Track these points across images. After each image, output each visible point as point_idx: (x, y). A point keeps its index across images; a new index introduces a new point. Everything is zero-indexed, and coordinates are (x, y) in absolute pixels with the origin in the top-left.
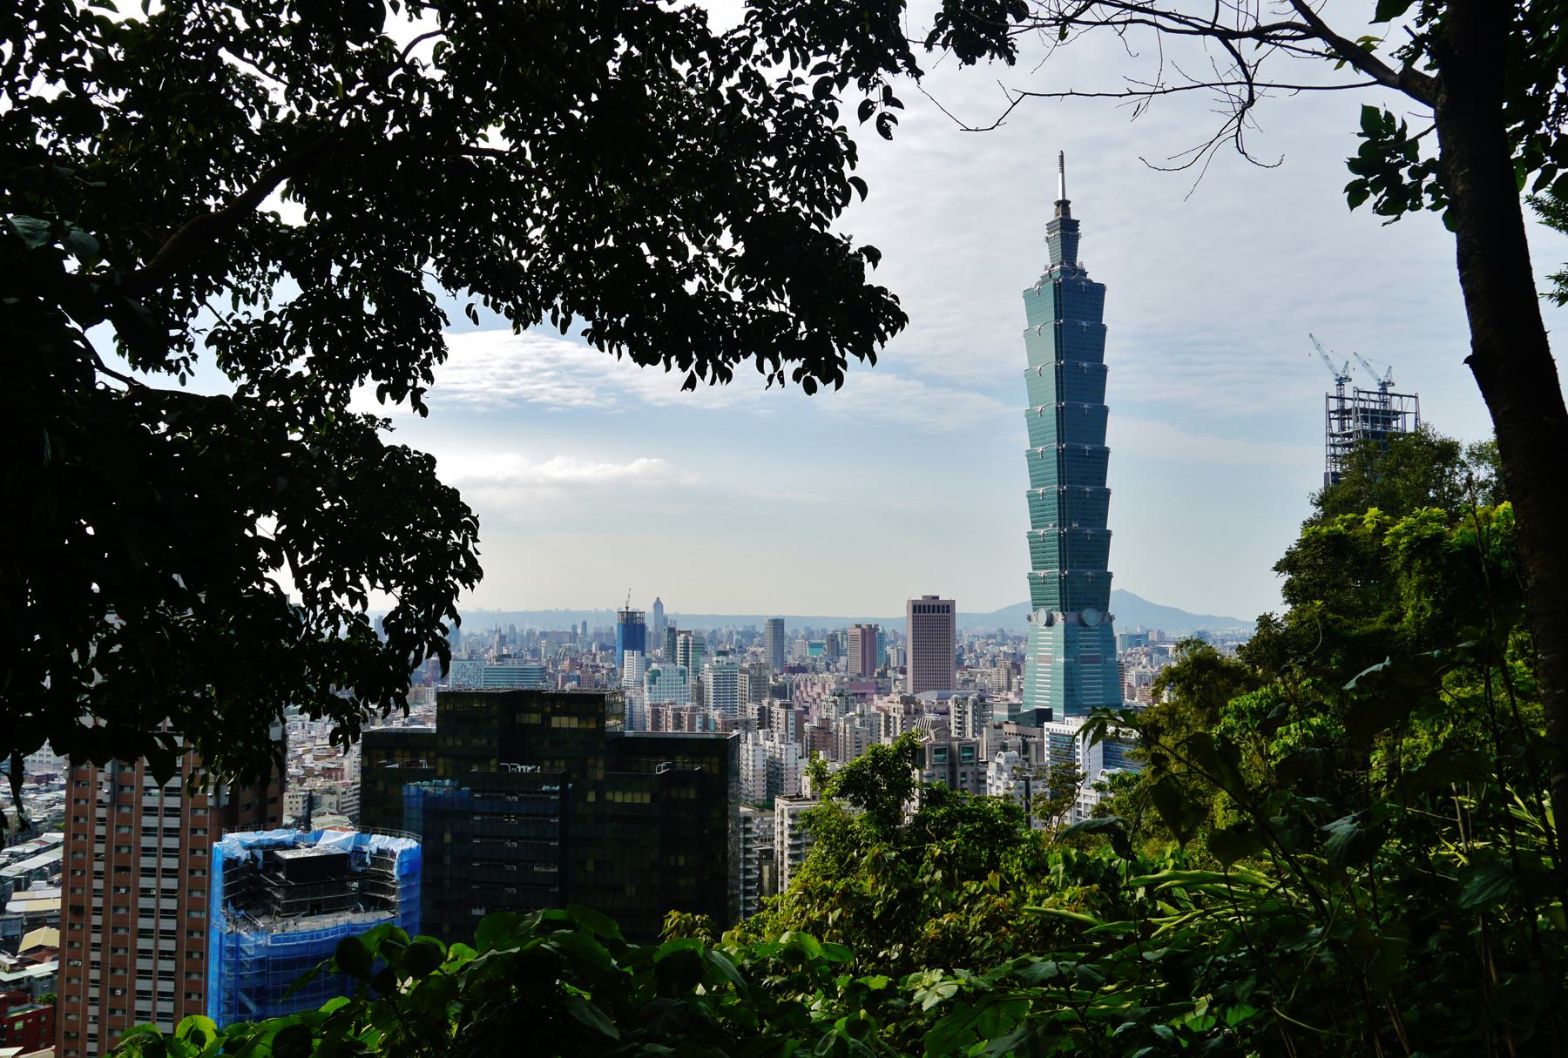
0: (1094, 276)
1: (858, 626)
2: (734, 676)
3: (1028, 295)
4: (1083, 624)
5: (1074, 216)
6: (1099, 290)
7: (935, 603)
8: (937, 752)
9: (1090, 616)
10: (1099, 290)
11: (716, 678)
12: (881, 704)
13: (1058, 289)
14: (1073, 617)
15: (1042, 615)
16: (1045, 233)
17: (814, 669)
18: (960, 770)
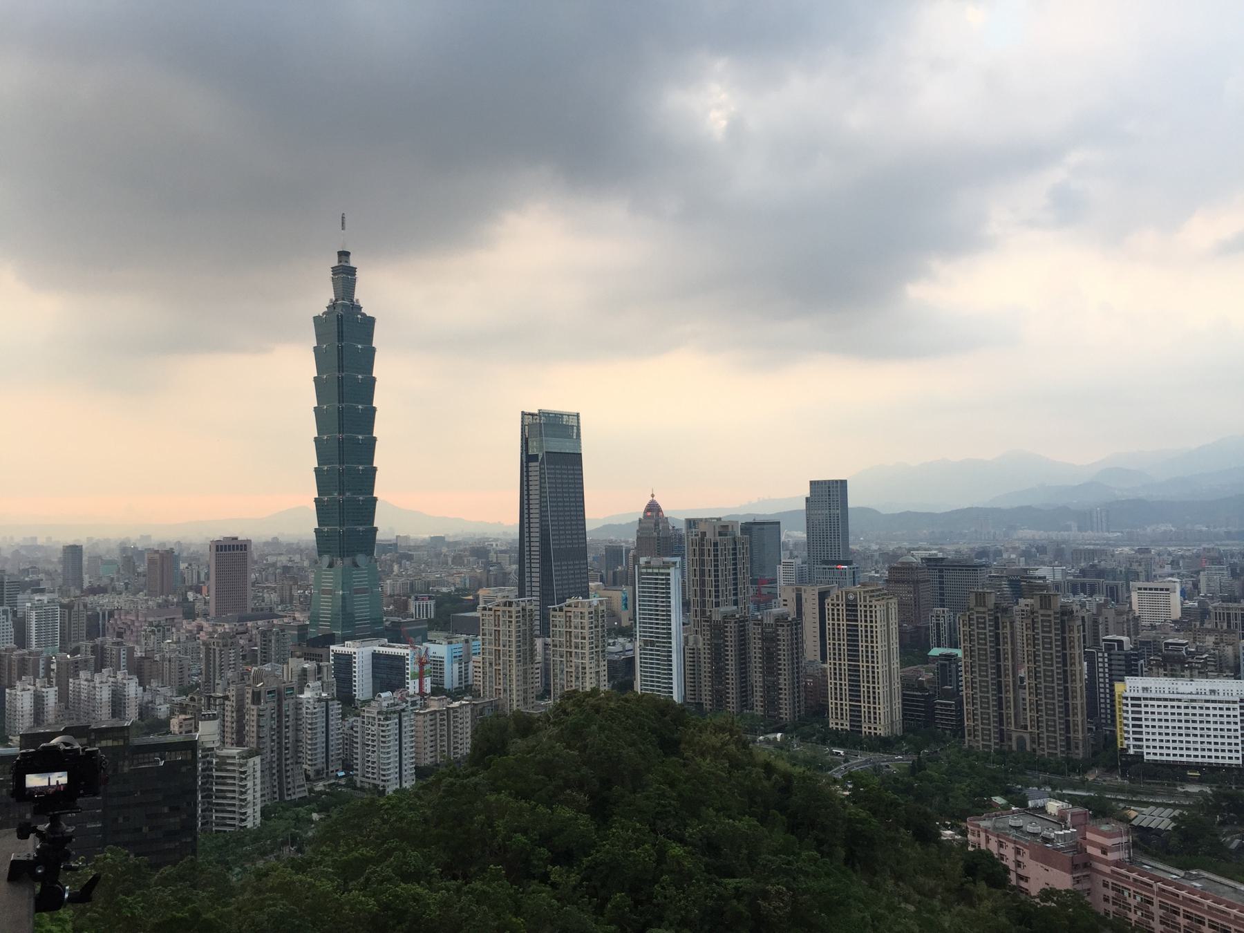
0: (367, 310)
1: (157, 552)
2: (54, 611)
3: (317, 320)
4: (356, 565)
5: (352, 264)
6: (370, 322)
7: (234, 543)
8: (269, 693)
9: (361, 559)
10: (370, 322)
11: (38, 615)
12: (189, 628)
13: (340, 320)
14: (348, 561)
15: (326, 559)
16: (330, 274)
17: (114, 589)
18: (285, 702)
